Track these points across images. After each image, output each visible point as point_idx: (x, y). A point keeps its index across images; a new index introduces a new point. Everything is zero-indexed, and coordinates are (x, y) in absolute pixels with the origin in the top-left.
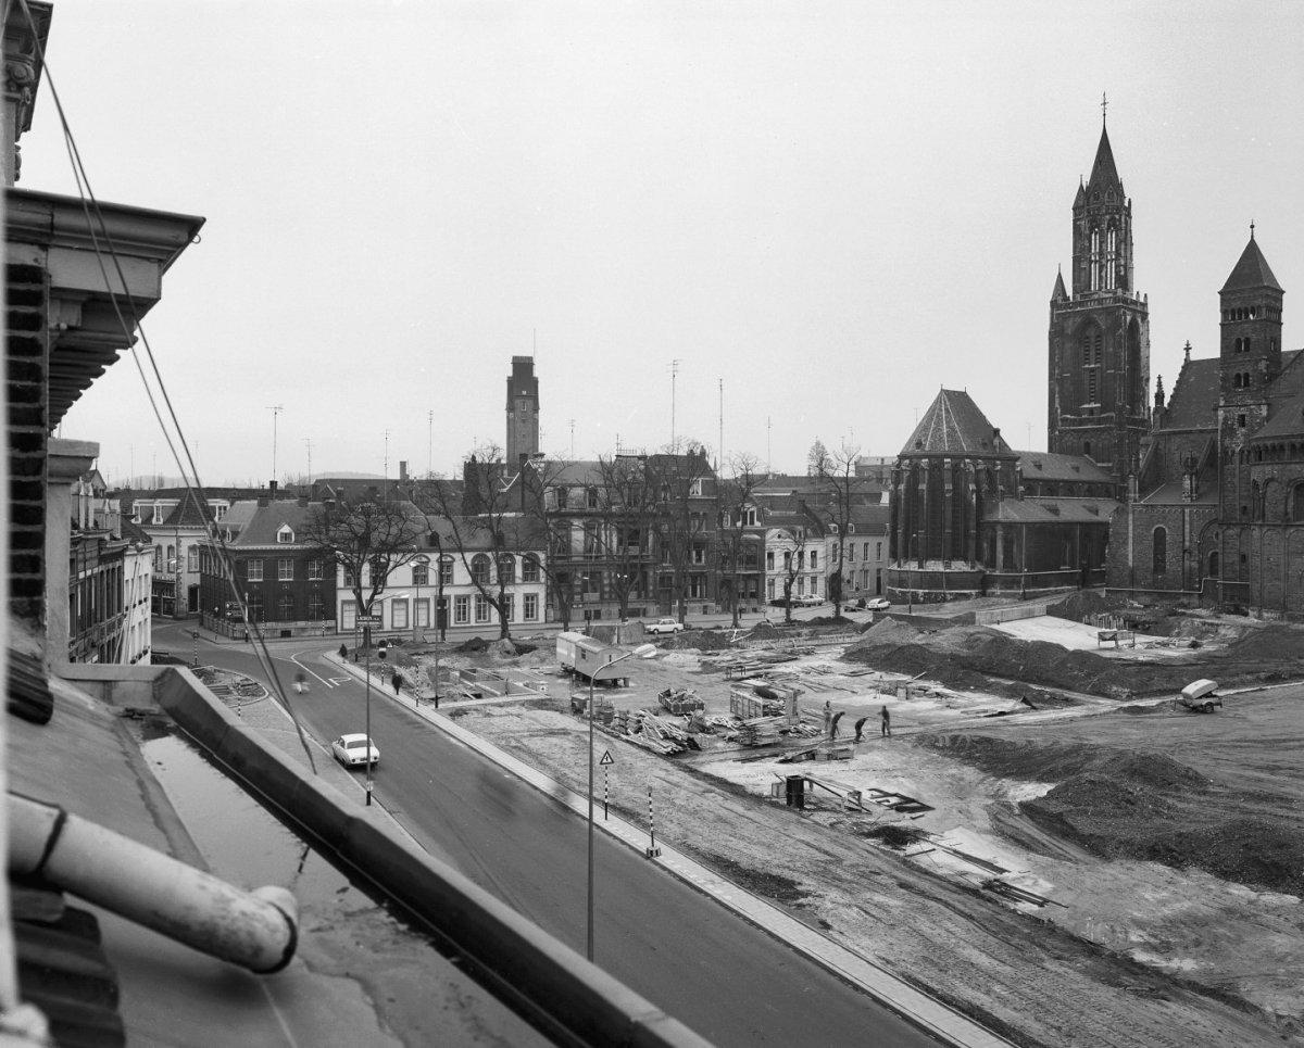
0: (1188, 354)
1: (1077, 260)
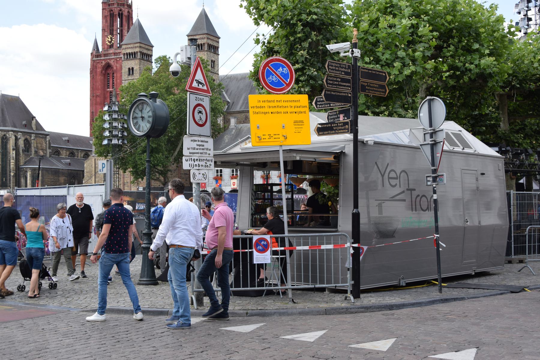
1: (104, 30)
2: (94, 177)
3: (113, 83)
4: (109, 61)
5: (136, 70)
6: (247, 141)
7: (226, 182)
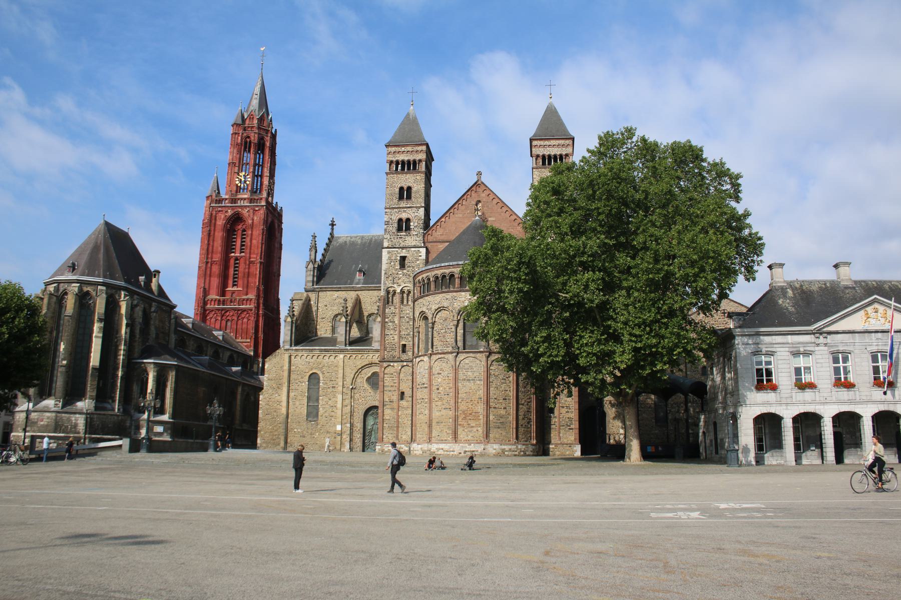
2: (285, 389)
4: (240, 210)
5: (417, 192)
6: (870, 309)
7: (825, 395)
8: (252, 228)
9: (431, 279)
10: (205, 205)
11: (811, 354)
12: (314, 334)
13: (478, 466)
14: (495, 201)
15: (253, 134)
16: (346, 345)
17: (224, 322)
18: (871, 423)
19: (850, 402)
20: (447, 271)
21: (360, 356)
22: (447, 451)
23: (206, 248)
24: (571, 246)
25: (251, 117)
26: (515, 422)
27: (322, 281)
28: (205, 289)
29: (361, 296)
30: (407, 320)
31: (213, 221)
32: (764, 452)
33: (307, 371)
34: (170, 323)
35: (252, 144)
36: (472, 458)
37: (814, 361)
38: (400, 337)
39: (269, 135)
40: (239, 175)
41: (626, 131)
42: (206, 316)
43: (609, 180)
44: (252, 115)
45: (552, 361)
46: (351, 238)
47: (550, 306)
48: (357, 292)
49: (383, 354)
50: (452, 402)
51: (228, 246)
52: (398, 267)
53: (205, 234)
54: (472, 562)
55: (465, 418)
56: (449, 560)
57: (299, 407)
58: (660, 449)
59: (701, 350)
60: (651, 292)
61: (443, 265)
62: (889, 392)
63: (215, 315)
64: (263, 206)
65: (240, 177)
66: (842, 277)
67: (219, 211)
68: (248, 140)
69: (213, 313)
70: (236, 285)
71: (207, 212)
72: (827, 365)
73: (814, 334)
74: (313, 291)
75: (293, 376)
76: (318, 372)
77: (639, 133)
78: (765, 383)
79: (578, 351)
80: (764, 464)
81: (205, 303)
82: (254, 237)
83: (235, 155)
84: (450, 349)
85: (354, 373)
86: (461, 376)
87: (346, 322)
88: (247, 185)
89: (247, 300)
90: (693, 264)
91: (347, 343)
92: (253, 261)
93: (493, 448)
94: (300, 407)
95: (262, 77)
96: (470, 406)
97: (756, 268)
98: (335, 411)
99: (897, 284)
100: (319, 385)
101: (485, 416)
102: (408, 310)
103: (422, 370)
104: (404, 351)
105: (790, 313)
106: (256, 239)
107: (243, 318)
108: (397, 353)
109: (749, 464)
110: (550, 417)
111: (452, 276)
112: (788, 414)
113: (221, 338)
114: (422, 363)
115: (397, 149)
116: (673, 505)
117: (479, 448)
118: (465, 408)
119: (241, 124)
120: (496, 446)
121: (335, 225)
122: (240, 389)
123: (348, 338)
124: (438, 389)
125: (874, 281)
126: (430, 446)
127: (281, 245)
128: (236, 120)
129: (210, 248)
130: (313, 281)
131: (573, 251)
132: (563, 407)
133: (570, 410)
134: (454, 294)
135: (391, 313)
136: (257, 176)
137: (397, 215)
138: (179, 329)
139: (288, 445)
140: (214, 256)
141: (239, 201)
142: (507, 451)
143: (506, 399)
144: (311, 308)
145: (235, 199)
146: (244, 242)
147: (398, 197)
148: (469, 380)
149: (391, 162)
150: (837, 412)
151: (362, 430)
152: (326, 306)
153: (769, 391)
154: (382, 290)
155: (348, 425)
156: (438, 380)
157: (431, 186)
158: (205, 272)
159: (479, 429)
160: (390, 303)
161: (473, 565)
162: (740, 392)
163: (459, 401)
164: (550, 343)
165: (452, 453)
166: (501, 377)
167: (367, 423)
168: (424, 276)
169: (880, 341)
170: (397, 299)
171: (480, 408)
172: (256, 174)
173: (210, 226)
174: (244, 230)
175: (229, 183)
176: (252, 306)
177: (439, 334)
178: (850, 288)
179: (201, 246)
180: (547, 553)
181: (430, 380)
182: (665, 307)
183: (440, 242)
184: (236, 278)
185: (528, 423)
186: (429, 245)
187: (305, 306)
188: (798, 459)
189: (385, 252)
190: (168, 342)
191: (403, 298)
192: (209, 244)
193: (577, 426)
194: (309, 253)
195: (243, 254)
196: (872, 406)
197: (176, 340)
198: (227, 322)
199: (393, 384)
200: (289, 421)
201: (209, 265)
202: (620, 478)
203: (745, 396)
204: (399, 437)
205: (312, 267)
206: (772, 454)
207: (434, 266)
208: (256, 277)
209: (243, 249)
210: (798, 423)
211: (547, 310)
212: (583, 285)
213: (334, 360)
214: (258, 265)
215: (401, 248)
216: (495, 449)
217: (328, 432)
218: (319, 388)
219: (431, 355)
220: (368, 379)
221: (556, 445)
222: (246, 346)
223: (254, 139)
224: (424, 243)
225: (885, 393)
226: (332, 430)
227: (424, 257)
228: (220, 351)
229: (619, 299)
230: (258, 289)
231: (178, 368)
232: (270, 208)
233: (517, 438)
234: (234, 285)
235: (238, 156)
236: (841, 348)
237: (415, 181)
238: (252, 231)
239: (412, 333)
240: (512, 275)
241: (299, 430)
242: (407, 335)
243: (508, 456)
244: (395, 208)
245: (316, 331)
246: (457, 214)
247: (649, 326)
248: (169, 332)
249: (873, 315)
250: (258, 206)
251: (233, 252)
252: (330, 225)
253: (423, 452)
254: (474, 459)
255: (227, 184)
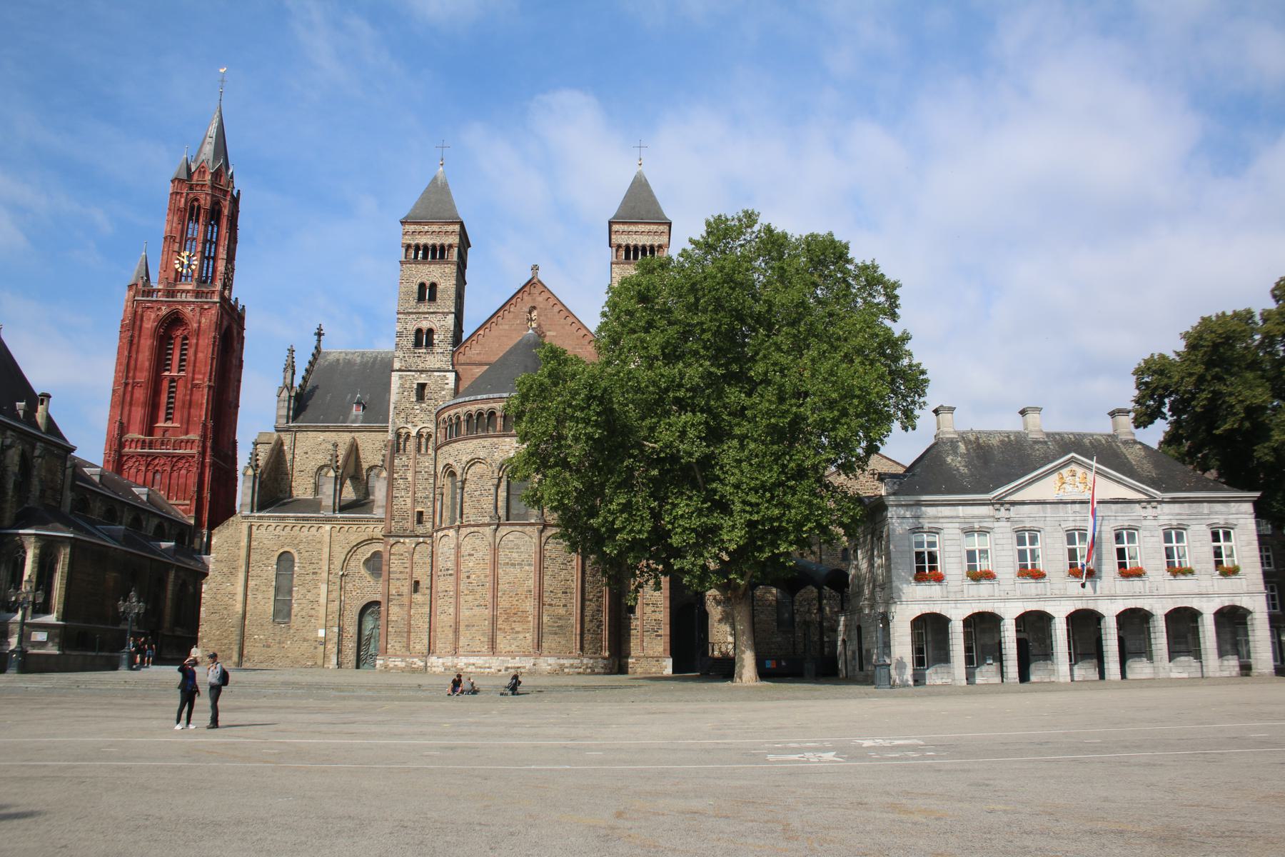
0: (319, 341)
2: (241, 576)
3: (182, 360)
4: (180, 307)
6: (1065, 472)
7: (1007, 588)
8: (198, 335)
9: (462, 418)
10: (126, 297)
11: (989, 532)
12: (287, 495)
13: (525, 690)
14: (557, 308)
15: (203, 196)
16: (334, 511)
17: (150, 475)
18: (1065, 626)
19: (1039, 598)
20: (485, 407)
21: (355, 527)
22: (481, 668)
23: (125, 362)
24: (662, 376)
25: (201, 170)
26: (579, 626)
27: (301, 417)
28: (121, 423)
29: (358, 440)
30: (426, 476)
31: (138, 323)
32: (926, 667)
33: (275, 548)
34: (64, 474)
35: (202, 211)
36: (516, 677)
37: (993, 546)
38: (415, 501)
39: (229, 198)
40: (179, 255)
41: (745, 216)
42: (123, 465)
43: (718, 284)
44: (203, 167)
45: (634, 539)
46: (346, 354)
47: (632, 460)
48: (353, 434)
49: (389, 527)
50: (489, 596)
51: (160, 361)
52: (414, 399)
53: (124, 341)
54: (511, 830)
55: (507, 620)
56: (478, 828)
57: (262, 603)
58: (783, 664)
59: (841, 525)
60: (773, 443)
61: (479, 397)
62: (1088, 584)
63: (137, 463)
64: (216, 303)
65: (182, 259)
66: (1031, 428)
67: (148, 308)
68: (196, 204)
69: (134, 460)
70: (170, 419)
71: (129, 309)
72: (1010, 547)
73: (993, 504)
74: (287, 431)
75: (254, 557)
76: (292, 551)
77: (763, 221)
78: (927, 571)
79: (670, 527)
80: (925, 684)
81: (121, 445)
82: (200, 348)
83: (174, 225)
84: (487, 520)
85: (346, 552)
86: (502, 558)
87: (336, 477)
88: (193, 271)
89: (188, 441)
90: (831, 405)
91: (337, 508)
92: (197, 384)
93: (547, 663)
94: (264, 603)
95: (220, 111)
96: (515, 603)
97: (917, 412)
98: (317, 608)
99: (1100, 438)
100: (293, 571)
101: (537, 617)
102: (427, 462)
103: (446, 549)
104: (420, 521)
105: (961, 475)
106: (203, 352)
107: (180, 469)
108: (410, 524)
109: (905, 685)
110: (630, 618)
111: (492, 414)
112: (957, 615)
113: (144, 498)
114: (446, 539)
115: (418, 228)
116: (798, 742)
117: (527, 663)
118: (508, 605)
119: (186, 180)
120: (551, 660)
121: (323, 334)
122: (172, 575)
123: (337, 501)
124: (468, 577)
125: (1072, 434)
126: (456, 661)
127: (241, 362)
128: (179, 173)
129: (133, 362)
130: (288, 417)
131: (665, 382)
132: (648, 604)
133: (658, 609)
134: (495, 439)
135: (403, 466)
136: (208, 258)
137: (414, 323)
138: (78, 483)
139: (245, 659)
140: (138, 374)
141: (179, 294)
142: (567, 668)
143: (566, 593)
144: (284, 455)
145: (174, 291)
146: (185, 355)
147: (416, 298)
148: (513, 565)
149: (408, 247)
150: (1022, 611)
151: (356, 637)
152: (306, 453)
153: (932, 583)
154: (390, 429)
155: (336, 629)
156: (469, 564)
157: (465, 283)
158: (122, 398)
159: (527, 635)
160: (401, 452)
161: (512, 834)
162: (894, 584)
163: (500, 594)
164: (631, 515)
165: (488, 670)
166: (560, 560)
167: (363, 627)
168: (452, 412)
169: (1078, 515)
170: (411, 445)
171: (530, 606)
172: (207, 255)
173: (133, 329)
174: (186, 338)
175: (164, 266)
176: (194, 451)
177: (471, 497)
178: (1041, 442)
179: (118, 359)
180: (619, 815)
181: (457, 564)
182: (792, 465)
183: (474, 364)
184: (171, 408)
185: (598, 627)
186: (457, 367)
187: (275, 452)
188: (970, 677)
189: (395, 377)
190: (60, 502)
191: (420, 444)
192: (130, 357)
193: (668, 632)
194: (283, 374)
195: (182, 374)
196: (1067, 603)
197: (72, 500)
198: (154, 473)
199: (402, 570)
200: (247, 622)
201: (130, 388)
202: (726, 705)
203: (901, 590)
204: (411, 647)
205: (288, 395)
206: (936, 670)
207: (467, 399)
208: (201, 408)
209: (184, 366)
210: (971, 627)
211: (627, 466)
212: (679, 431)
213: (316, 533)
214: (206, 390)
215: (418, 371)
216: (550, 665)
217: (305, 640)
218: (293, 574)
219: (459, 527)
220: (367, 562)
221: (638, 658)
222: (183, 511)
223: (205, 204)
224: (453, 365)
225: (1083, 586)
226: (311, 636)
227: (452, 385)
228: (142, 517)
229: (729, 452)
230: (205, 426)
231: (74, 543)
232: (227, 307)
233: (582, 648)
234: (167, 420)
235: (180, 226)
236: (1028, 525)
237: (443, 275)
238: (198, 340)
239: (432, 495)
240: (578, 414)
241: (261, 637)
242: (425, 498)
243: (568, 674)
244: (412, 313)
245: (291, 491)
246: (502, 324)
247: (770, 490)
248: (63, 487)
249: (1069, 479)
250: (207, 302)
251: (168, 370)
252: (315, 334)
253: (445, 669)
254: (520, 679)
255: (162, 268)
